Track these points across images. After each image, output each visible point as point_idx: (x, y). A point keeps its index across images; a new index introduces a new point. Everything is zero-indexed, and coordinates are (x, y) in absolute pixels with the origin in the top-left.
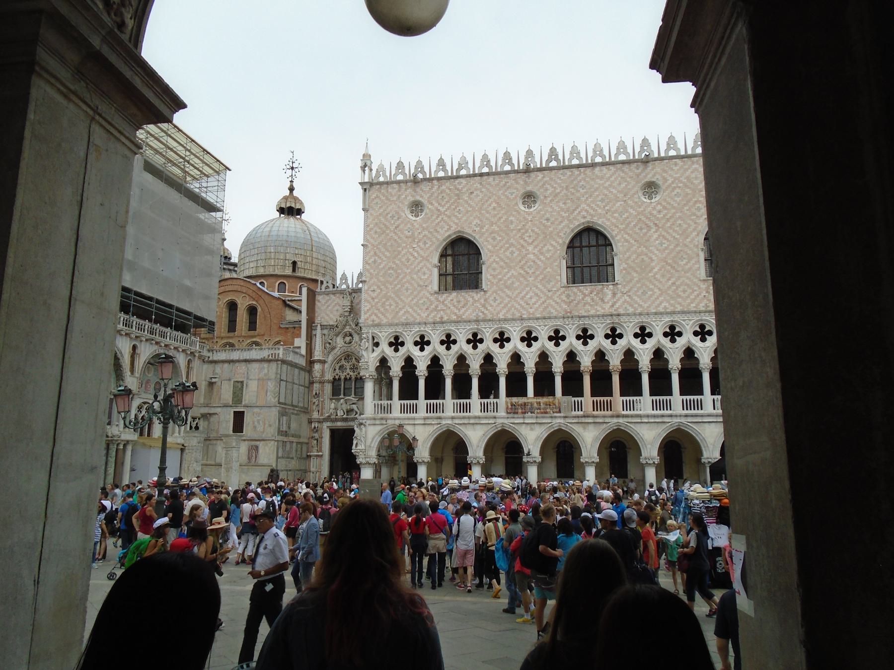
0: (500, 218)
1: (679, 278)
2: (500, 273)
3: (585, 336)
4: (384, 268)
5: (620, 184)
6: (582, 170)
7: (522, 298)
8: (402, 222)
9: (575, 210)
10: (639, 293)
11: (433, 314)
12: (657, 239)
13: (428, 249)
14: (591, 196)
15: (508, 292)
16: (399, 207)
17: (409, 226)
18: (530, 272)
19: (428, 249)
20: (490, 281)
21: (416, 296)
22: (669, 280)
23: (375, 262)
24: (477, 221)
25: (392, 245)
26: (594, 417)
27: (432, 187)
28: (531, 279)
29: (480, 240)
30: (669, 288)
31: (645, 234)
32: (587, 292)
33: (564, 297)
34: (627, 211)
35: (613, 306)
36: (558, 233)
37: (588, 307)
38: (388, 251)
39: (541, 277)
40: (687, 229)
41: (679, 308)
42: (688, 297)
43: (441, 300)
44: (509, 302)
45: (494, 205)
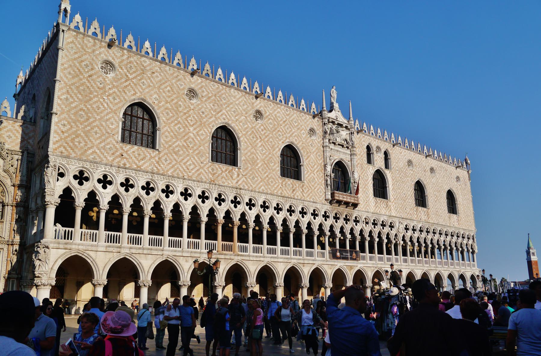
0: (173, 100)
1: (269, 174)
2: (170, 141)
3: (220, 200)
4: (75, 107)
5: (244, 105)
6: (224, 87)
7: (185, 164)
8: (95, 74)
9: (219, 112)
10: (251, 178)
11: (117, 160)
12: (260, 147)
13: (116, 104)
14: (228, 106)
15: (175, 156)
16: (93, 59)
17: (101, 79)
18: (191, 146)
19: (116, 104)
20: (163, 145)
21: (104, 141)
22: (265, 173)
23: (67, 99)
24: (155, 96)
25: (84, 90)
26: (225, 254)
27: (122, 56)
28: (191, 151)
29: (158, 111)
30: (265, 178)
31: (255, 141)
32: (224, 170)
33: (210, 169)
34: (247, 124)
35: (237, 182)
36: (209, 124)
37: (223, 180)
38: (80, 94)
39: (197, 152)
40: (273, 146)
41: (269, 192)
42: (273, 186)
43: (125, 149)
44: (176, 164)
45: (169, 88)
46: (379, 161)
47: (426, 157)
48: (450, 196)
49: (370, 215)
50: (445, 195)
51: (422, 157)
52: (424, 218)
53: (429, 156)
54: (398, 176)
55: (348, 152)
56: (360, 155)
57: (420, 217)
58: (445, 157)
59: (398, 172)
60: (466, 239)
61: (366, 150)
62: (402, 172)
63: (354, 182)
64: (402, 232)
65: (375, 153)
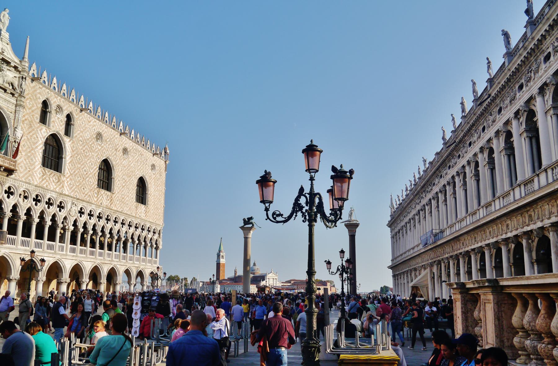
46: (57, 124)
47: (121, 134)
48: (142, 184)
49: (31, 188)
50: (135, 182)
51: (116, 134)
52: (105, 202)
53: (124, 133)
54: (81, 147)
55: (13, 100)
56: (30, 109)
57: (101, 201)
58: (144, 139)
59: (81, 143)
60: (151, 233)
61: (40, 106)
62: (87, 144)
63: (15, 142)
64: (74, 215)
65: (53, 112)
